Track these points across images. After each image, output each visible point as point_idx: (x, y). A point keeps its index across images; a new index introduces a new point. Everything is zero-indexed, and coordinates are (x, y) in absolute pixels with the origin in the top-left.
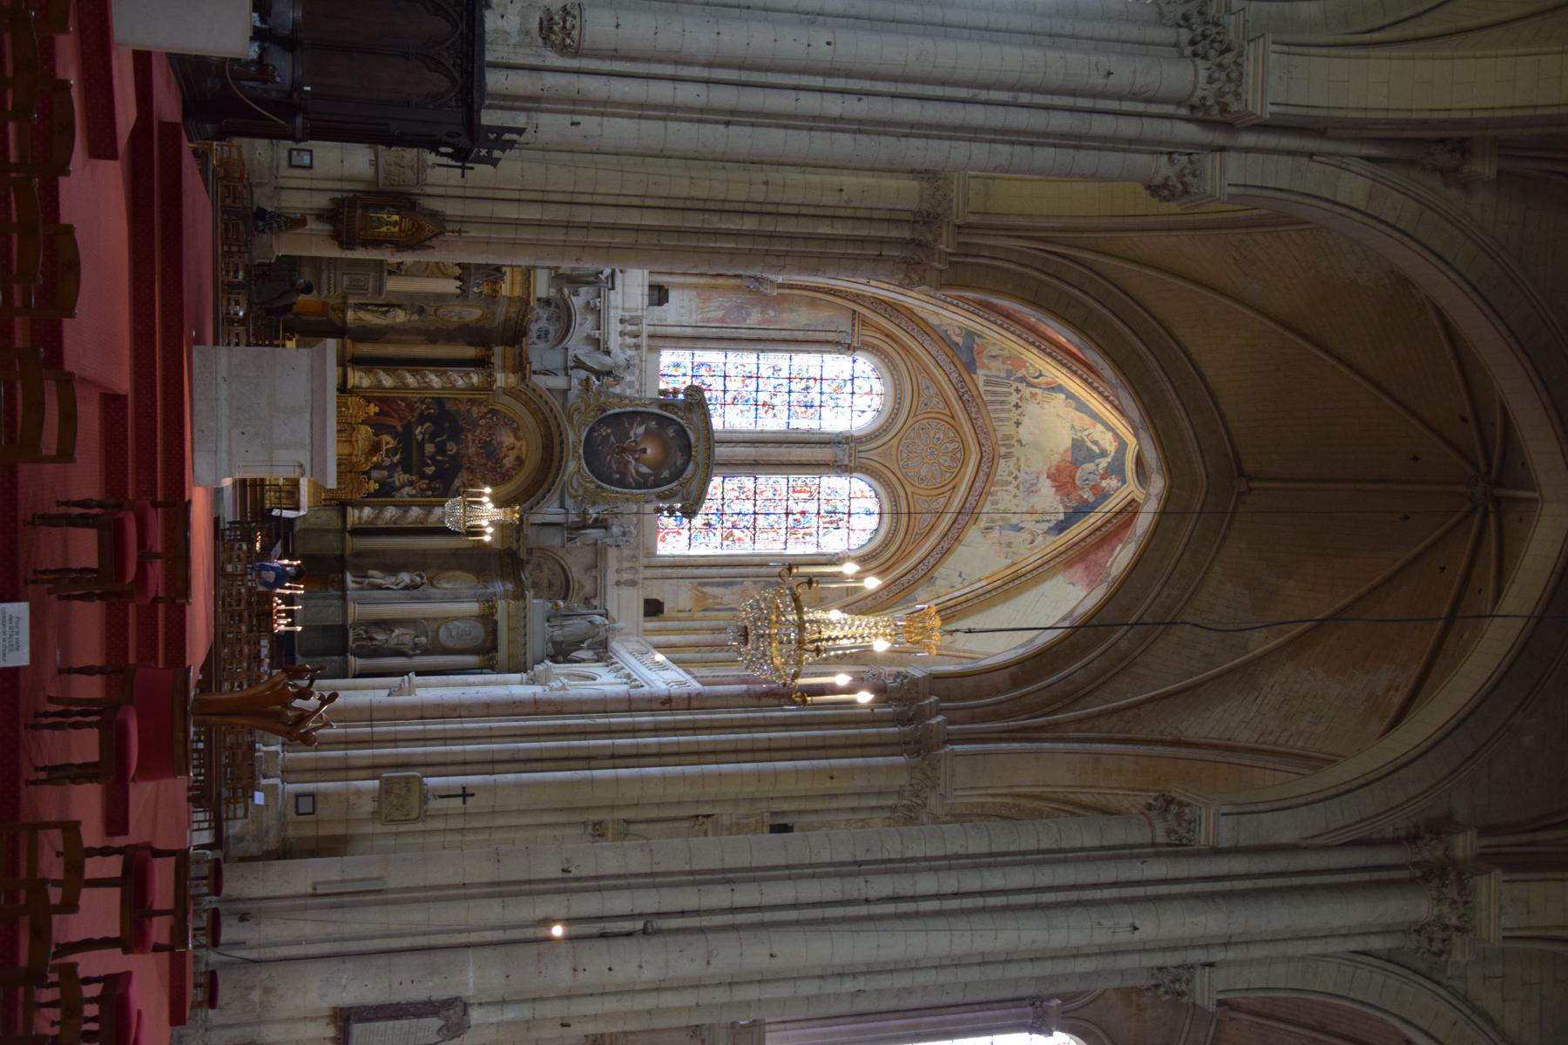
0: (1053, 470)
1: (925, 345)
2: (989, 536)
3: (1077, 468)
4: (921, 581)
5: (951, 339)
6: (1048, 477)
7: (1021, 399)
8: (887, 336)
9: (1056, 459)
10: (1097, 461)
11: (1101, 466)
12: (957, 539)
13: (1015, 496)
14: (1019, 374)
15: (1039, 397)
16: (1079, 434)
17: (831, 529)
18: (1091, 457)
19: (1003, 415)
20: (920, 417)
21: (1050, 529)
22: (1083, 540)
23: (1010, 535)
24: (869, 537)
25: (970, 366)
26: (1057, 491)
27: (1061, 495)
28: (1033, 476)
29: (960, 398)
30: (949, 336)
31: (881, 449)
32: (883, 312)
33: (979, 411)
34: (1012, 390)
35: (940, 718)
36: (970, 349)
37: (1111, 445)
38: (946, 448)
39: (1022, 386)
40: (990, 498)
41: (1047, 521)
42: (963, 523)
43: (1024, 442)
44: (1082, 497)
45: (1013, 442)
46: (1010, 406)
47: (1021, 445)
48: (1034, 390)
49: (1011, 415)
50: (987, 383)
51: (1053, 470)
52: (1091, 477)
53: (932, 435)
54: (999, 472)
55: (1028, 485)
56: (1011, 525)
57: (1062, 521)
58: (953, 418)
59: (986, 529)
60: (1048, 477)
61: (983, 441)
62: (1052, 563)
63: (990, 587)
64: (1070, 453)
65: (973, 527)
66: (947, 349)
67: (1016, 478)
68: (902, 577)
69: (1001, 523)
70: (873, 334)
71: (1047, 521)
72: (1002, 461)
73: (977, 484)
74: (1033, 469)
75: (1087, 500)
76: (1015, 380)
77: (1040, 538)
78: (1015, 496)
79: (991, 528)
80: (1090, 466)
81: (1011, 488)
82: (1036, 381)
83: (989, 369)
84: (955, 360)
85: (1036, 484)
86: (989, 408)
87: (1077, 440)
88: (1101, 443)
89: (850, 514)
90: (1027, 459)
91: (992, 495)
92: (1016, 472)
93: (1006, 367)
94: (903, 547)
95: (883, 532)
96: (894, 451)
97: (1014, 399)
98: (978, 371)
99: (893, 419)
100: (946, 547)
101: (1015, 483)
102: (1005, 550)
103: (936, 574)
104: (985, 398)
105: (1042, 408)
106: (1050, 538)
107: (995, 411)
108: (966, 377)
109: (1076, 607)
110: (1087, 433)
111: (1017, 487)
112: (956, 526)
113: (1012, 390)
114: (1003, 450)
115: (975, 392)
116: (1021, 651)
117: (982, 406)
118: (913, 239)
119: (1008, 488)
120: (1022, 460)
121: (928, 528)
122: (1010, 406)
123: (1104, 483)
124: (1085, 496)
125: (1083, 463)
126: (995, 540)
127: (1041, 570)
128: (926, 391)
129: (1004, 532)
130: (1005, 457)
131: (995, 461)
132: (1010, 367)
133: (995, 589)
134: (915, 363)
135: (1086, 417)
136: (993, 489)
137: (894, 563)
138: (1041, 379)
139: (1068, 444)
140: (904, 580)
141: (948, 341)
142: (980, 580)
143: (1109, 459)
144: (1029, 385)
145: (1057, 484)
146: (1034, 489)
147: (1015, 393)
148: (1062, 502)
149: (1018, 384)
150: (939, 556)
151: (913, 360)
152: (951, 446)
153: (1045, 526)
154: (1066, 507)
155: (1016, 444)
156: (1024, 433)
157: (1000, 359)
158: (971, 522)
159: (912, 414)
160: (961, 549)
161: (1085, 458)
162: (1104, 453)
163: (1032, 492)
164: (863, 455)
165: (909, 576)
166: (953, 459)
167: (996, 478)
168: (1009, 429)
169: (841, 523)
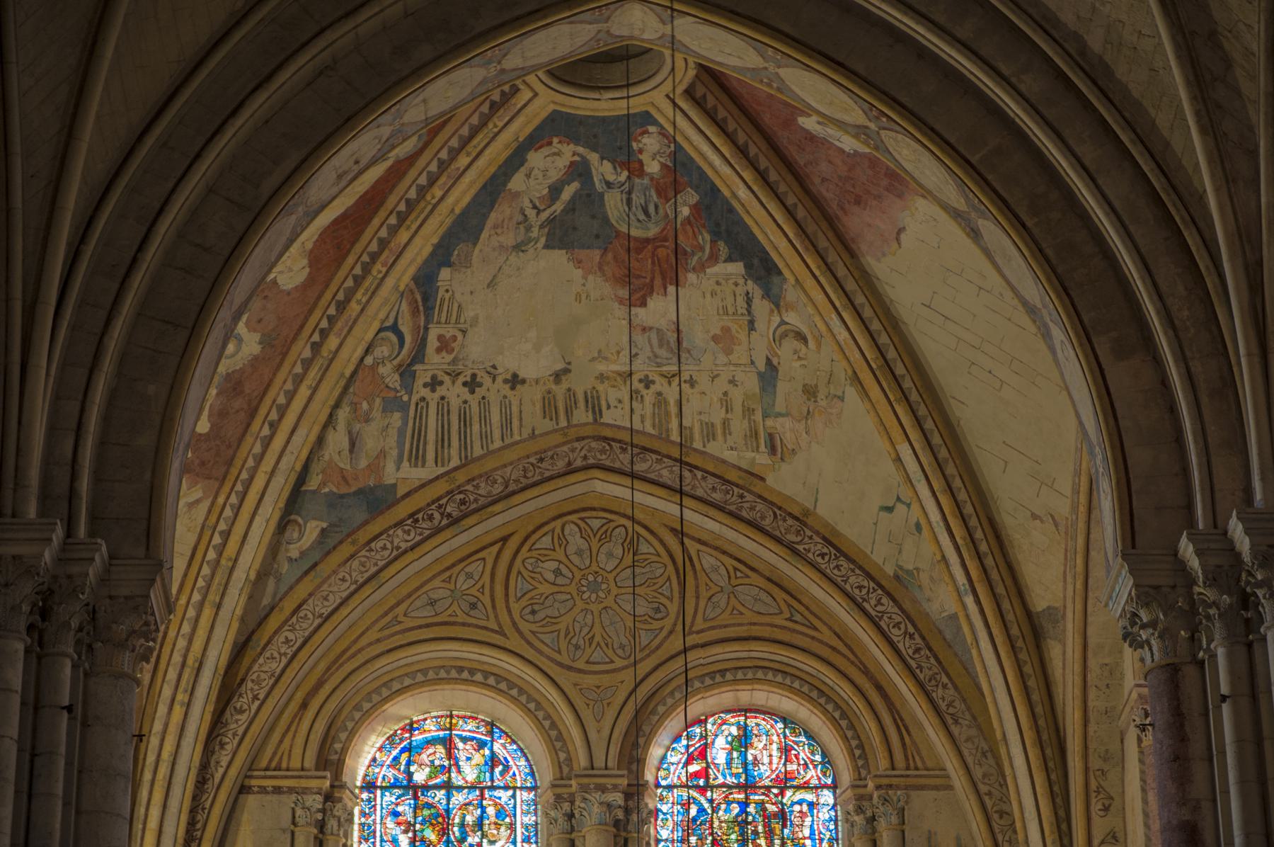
0: (624, 293)
1: (326, 611)
2: (789, 438)
4: (907, 606)
5: (311, 548)
6: (643, 304)
7: (455, 375)
8: (304, 706)
9: (599, 287)
10: (599, 186)
11: (611, 178)
12: (802, 519)
14: (394, 380)
15: (449, 332)
17: (786, 831)
18: (589, 200)
19: (495, 418)
20: (504, 617)
21: (767, 295)
22: (790, 212)
24: (803, 739)
27: (687, 271)
28: (639, 338)
29: (456, 521)
30: (303, 554)
31: (586, 714)
32: (244, 717)
33: (487, 476)
34: (433, 398)
35: (1236, 529)
36: (335, 501)
37: (558, 154)
38: (579, 553)
39: (423, 376)
40: (697, 445)
41: (749, 301)
42: (760, 506)
43: (560, 366)
44: (688, 221)
45: (559, 391)
46: (474, 401)
47: (566, 371)
48: (432, 342)
49: (493, 398)
50: (417, 458)
52: (637, 199)
53: (545, 589)
55: (663, 353)
56: (763, 389)
57: (748, 267)
58: (505, 539)
59: (773, 450)
60: (643, 304)
61: (561, 465)
62: (851, 285)
63: (914, 435)
64: (582, 254)
65: (770, 481)
66: (335, 559)
67: (648, 383)
68: (897, 652)
69: (758, 416)
70: (300, 740)
71: (749, 301)
72: (608, 417)
75: (695, 208)
76: (410, 393)
77: (791, 318)
79: (771, 437)
80: (613, 204)
81: (671, 394)
82: (408, 339)
83: (383, 454)
84: (363, 536)
85: (659, 330)
86: (478, 451)
87: (550, 236)
88: (554, 176)
89: (748, 786)
94: (826, 653)
95: (788, 704)
96: (590, 680)
97: (455, 393)
98: (389, 480)
99: (512, 685)
100: (820, 547)
101: (660, 385)
102: (823, 403)
103: (890, 570)
104: (455, 462)
106: (791, 294)
107: (485, 437)
108: (402, 510)
109: (945, 207)
110: (531, 213)
112: (767, 523)
114: (582, 415)
115: (441, 488)
116: (1058, 334)
117: (475, 470)
118: (31, 628)
120: (601, 367)
121: (776, 591)
122: (474, 401)
123: (653, 167)
124: (685, 211)
125: (606, 220)
126: (801, 426)
127: (867, 313)
128: (439, 607)
129: (780, 406)
130: (597, 411)
131: (608, 433)
132: (378, 401)
133: (919, 422)
134: (372, 635)
135: (493, 217)
136: (675, 437)
137: (866, 672)
138: (405, 329)
139: (559, 256)
140: (905, 646)
141: (316, 556)
142: (898, 460)
143: (593, 157)
144: (419, 355)
147: (441, 391)
148: (701, 268)
149: (419, 382)
150: (842, 562)
151: (363, 642)
152: (576, 541)
153: (761, 307)
154: (714, 258)
155: (565, 385)
157: (357, 427)
158: (758, 487)
159: (497, 639)
160: (822, 511)
162: (580, 171)
164: (599, 762)
165: (895, 634)
166: (606, 537)
168: (530, 397)
169: (771, 808)
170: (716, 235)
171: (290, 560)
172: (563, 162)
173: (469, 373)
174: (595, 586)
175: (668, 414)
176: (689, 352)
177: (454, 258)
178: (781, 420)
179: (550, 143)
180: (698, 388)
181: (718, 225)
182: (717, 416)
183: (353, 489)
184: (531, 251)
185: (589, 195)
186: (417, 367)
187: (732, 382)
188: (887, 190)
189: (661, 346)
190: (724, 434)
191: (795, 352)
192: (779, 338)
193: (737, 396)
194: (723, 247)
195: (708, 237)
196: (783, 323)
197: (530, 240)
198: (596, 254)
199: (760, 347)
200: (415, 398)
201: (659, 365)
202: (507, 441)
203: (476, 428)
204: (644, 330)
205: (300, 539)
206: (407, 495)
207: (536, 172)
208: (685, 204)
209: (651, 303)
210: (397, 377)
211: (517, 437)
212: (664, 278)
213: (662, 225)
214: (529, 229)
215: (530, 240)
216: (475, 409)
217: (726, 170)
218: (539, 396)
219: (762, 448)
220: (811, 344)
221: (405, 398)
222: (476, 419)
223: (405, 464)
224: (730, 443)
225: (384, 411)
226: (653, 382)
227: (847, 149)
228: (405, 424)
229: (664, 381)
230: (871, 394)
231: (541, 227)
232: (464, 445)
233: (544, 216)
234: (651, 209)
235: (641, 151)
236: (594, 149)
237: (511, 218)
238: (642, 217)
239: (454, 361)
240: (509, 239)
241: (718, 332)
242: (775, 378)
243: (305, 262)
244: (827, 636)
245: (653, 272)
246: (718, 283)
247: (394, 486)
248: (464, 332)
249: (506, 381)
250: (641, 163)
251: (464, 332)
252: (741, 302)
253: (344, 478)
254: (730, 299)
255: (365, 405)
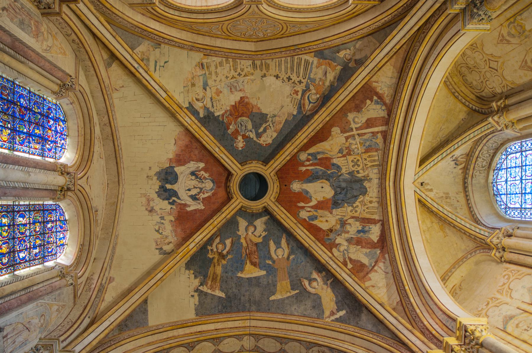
0: (246, 100)
2: (198, 69)
3: (248, 117)
5: (343, 50)
9: (253, 102)
10: (253, 130)
11: (250, 133)
13: (227, 77)
14: (312, 87)
15: (295, 96)
16: (270, 119)
18: (256, 127)
19: (283, 67)
21: (208, 109)
23: (200, 83)
25: (320, 54)
26: (233, 106)
27: (230, 110)
28: (241, 87)
30: (346, 49)
34: (301, 78)
36: (334, 59)
37: (264, 141)
39: (303, 85)
40: (224, 59)
41: (213, 106)
43: (264, 79)
44: (230, 124)
45: (264, 71)
47: (262, 77)
48: (300, 94)
50: (307, 62)
51: (246, 100)
52: (244, 128)
54: (243, 62)
55: (235, 84)
56: (207, 81)
59: (202, 64)
60: (241, 98)
64: (257, 111)
67: (239, 75)
71: (213, 106)
72: (250, 62)
73: (233, 54)
74: (246, 87)
75: (228, 128)
76: (307, 81)
77: (201, 104)
78: (227, 77)
79: (203, 68)
80: (250, 126)
81: (233, 73)
82: (306, 98)
85: (237, 91)
86: (289, 58)
87: (266, 118)
90: (253, 81)
91: (226, 61)
92: (243, 74)
93: (318, 80)
97: (294, 77)
100: (185, 47)
102: (190, 83)
103: (163, 45)
104: (296, 57)
105: (287, 97)
107: (286, 62)
110: (271, 125)
111: (233, 77)
113: (301, 78)
114: (258, 63)
119: (232, 70)
123: (240, 138)
124: (231, 127)
125: (252, 121)
130: (254, 63)
132: (317, 83)
135: (281, 126)
136: (231, 60)
138: (307, 101)
139: (264, 111)
141: (341, 47)
143: (255, 139)
144: (304, 92)
145: (237, 105)
146: (233, 90)
147: (298, 79)
148: (226, 112)
149: (304, 84)
153: (209, 105)
155: (263, 72)
156: (270, 80)
157: (324, 78)
161: (255, 122)
162: (259, 135)
163: (231, 89)
167: (238, 61)
168: (273, 70)
170: (223, 122)
171: (350, 50)
172: (263, 139)
173: (290, 82)
174: (254, 29)
175: (233, 66)
176: (228, 86)
177: (292, 117)
178: (201, 74)
179: (266, 144)
180: (225, 76)
181: (222, 125)
182: (219, 69)
183: (327, 60)
184: (271, 114)
185: (256, 128)
186: (305, 89)
187: (215, 81)
188: (180, 155)
189: (236, 86)
190: (217, 65)
191: (199, 95)
192: (204, 97)
193: (214, 77)
194: (221, 119)
195: (225, 121)
196: (203, 102)
197: (272, 117)
198: (254, 111)
199: (209, 93)
200: (306, 80)
201: (236, 80)
202: (280, 59)
203: (289, 66)
204: (241, 90)
205: (346, 54)
206: (311, 52)
207: (270, 137)
208: (231, 129)
209: (239, 98)
210: (311, 88)
211: (277, 60)
212: (236, 106)
213: (237, 122)
214: (272, 121)
215: (272, 117)
216: (289, 71)
217: (222, 155)
218: (270, 71)
219: (205, 64)
220: (194, 99)
221: (309, 81)
222: (289, 68)
223: (311, 62)
224: (215, 63)
225: (315, 80)
226: (238, 75)
227: (192, 162)
228: (310, 74)
229: (235, 76)
230: (176, 105)
231: (269, 121)
232: (293, 61)
233: (268, 124)
234: (240, 126)
235: (243, 142)
236: (255, 141)
237: (277, 125)
238: (242, 123)
239: (294, 87)
240: (277, 119)
241: (220, 94)
242: (204, 86)
243: (332, 133)
244: (179, 24)
245: (239, 108)
246: (221, 108)
247: (315, 56)
248: (291, 94)
249: (280, 77)
250: (243, 139)
251: (291, 94)
252: (215, 105)
253: (330, 65)
254: (218, 105)
255: (321, 83)
